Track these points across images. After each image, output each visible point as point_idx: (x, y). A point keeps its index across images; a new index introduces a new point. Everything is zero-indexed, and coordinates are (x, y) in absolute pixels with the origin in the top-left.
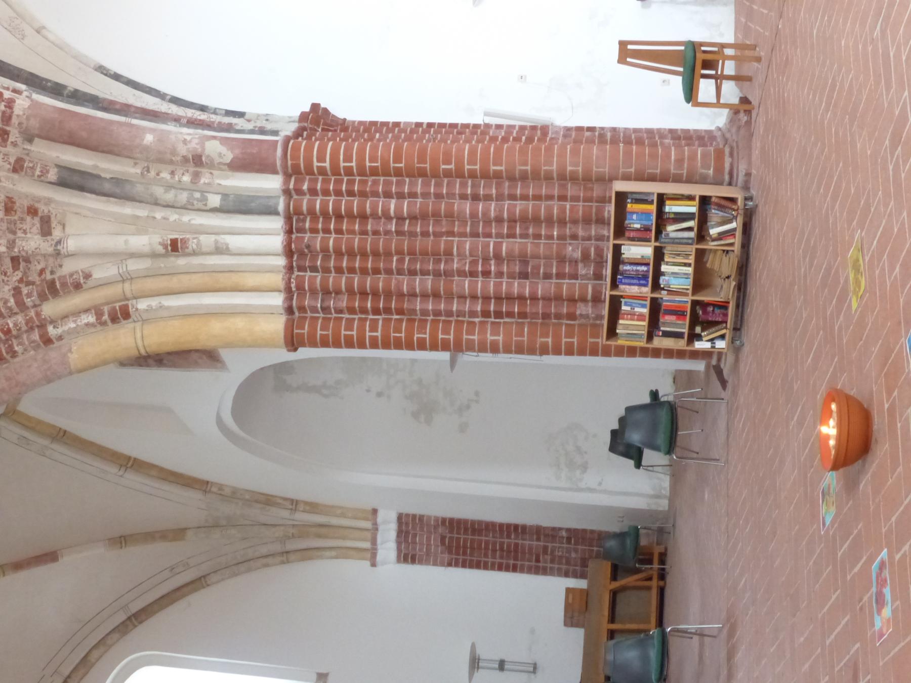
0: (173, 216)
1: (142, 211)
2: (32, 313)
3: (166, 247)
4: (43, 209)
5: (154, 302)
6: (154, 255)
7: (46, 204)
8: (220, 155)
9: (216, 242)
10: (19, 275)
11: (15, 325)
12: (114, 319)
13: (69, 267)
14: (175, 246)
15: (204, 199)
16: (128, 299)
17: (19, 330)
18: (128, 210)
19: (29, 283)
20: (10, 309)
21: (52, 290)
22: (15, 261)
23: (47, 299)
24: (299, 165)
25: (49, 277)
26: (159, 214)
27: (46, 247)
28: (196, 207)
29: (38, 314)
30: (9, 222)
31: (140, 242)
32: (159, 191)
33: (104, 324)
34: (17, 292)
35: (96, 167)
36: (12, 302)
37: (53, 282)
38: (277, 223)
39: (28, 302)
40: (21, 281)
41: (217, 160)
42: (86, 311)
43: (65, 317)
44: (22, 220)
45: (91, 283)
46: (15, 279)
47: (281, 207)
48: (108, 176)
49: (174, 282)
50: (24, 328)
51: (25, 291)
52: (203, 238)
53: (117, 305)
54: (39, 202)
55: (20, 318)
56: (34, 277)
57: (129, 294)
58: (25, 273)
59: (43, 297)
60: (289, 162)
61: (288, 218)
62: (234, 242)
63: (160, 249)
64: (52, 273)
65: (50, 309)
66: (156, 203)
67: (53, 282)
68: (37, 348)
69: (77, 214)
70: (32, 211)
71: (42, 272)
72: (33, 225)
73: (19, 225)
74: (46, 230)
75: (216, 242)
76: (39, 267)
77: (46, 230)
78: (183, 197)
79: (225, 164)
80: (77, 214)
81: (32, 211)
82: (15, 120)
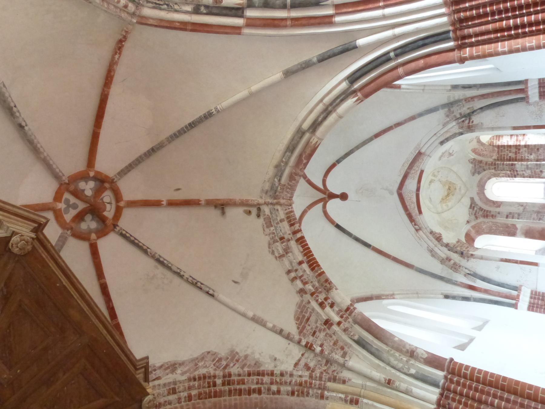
0: (393, 371)
1: (382, 364)
2: (323, 383)
3: (385, 380)
4: (346, 349)
5: (370, 402)
6: (378, 382)
7: (348, 348)
8: (422, 354)
9: (407, 387)
10: (325, 368)
11: (315, 383)
12: (351, 402)
13: (346, 374)
14: (389, 383)
15: (409, 369)
16: (360, 396)
17: (315, 385)
18: (377, 361)
19: (327, 373)
20: (316, 377)
21: (334, 379)
22: (327, 362)
23: (330, 382)
24: (455, 369)
25: (335, 374)
26: (388, 368)
27: (341, 360)
28: (404, 371)
29: (325, 384)
30: (333, 348)
31: (376, 375)
32: (392, 360)
33: (346, 401)
34: (322, 373)
35: (373, 341)
36: (318, 375)
37: (336, 376)
38: (438, 391)
39: (323, 379)
40: (325, 371)
41: (420, 355)
42: (342, 393)
43: (333, 391)
44: (337, 349)
45: (350, 383)
46: (323, 369)
47: (441, 383)
48: (375, 347)
49: (383, 398)
50: (317, 386)
51: (324, 374)
52: (402, 384)
53: (355, 397)
54: (346, 345)
55: (318, 382)
56: (330, 372)
57: (362, 394)
58: (328, 369)
59: (329, 380)
60: (451, 366)
61: (443, 389)
62: (415, 390)
63: (383, 380)
64: (337, 373)
65: (329, 384)
66: (388, 364)
67: (336, 376)
68: (317, 397)
69: (357, 356)
70: (342, 348)
71: (334, 371)
72: (341, 352)
73: (335, 350)
74: (344, 355)
75: (407, 387)
76: (334, 369)
77: (344, 355)
78: (401, 365)
79: (423, 358)
80: (357, 356)
81: (342, 348)
82: (353, 314)
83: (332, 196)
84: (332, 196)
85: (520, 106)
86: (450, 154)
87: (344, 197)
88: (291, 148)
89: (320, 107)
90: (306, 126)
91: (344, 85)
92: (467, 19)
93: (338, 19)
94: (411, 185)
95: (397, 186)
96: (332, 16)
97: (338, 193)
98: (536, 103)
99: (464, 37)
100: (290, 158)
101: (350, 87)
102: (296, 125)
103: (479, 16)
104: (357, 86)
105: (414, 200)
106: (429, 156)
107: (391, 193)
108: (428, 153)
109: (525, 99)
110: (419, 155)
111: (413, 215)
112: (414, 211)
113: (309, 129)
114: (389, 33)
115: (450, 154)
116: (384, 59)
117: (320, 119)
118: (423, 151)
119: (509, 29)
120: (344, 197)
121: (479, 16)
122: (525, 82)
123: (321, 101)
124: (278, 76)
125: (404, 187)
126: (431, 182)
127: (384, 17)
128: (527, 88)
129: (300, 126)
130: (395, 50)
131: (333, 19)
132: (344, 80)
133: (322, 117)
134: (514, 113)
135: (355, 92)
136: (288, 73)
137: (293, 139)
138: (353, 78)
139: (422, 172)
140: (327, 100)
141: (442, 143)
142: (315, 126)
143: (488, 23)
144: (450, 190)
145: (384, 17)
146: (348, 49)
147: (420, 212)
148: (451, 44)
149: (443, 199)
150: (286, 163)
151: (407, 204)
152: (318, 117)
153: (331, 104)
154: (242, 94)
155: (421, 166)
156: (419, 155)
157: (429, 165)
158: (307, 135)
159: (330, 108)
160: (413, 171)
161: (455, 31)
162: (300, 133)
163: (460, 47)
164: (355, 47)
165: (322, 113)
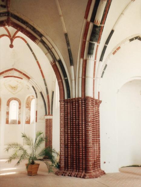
83: (12, 40)
84: (12, 40)
85: (45, 114)
86: (28, 89)
87: (11, 46)
88: (34, 29)
89: (50, 47)
90: (44, 39)
91: (58, 58)
92: (73, 104)
93: (82, 60)
94: (17, 74)
95: (16, 68)
96: (83, 58)
97: (13, 44)
98: (44, 118)
99: (67, 102)
100: (30, 28)
101: (57, 60)
102: (45, 35)
103: (73, 108)
104: (57, 63)
105: (10, 75)
106: (28, 81)
107: (13, 66)
108: (29, 81)
109: (46, 114)
110: (29, 78)
111: (3, 74)
112: (5, 75)
113: (42, 40)
114: (73, 78)
115: (28, 89)
116: (65, 75)
117: (46, 45)
118: (30, 79)
119: (67, 116)
120: (11, 46)
121: (73, 108)
122: (52, 115)
123: (53, 47)
124: (66, 31)
125: (16, 71)
126: (18, 81)
127: (79, 78)
128: (50, 115)
129: (44, 36)
130: (67, 79)
131: (82, 58)
132: (60, 59)
133: (47, 46)
134: (42, 111)
135: (55, 62)
136: (66, 35)
137: (38, 32)
138: (60, 62)
139: (22, 79)
140: (53, 50)
141: (33, 87)
142: (43, 42)
143: (70, 110)
144: (14, 88)
145: (79, 78)
146: (72, 63)
147: (5, 77)
148: (66, 98)
149: (10, 85)
150: (28, 26)
151: (8, 72)
152: (47, 45)
153: (51, 51)
154: (61, 13)
155: (24, 78)
156: (29, 78)
157: (25, 81)
158: (39, 39)
159: (50, 50)
160: (22, 75)
161: (70, 100)
162: (41, 35)
163: (64, 101)
164: (71, 65)
165: (48, 47)
